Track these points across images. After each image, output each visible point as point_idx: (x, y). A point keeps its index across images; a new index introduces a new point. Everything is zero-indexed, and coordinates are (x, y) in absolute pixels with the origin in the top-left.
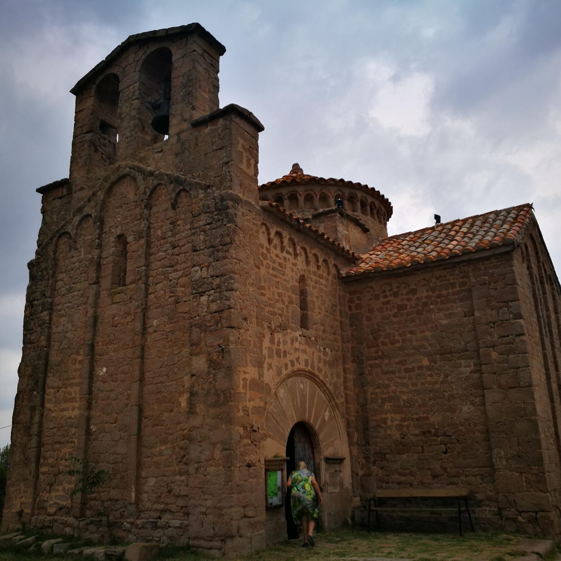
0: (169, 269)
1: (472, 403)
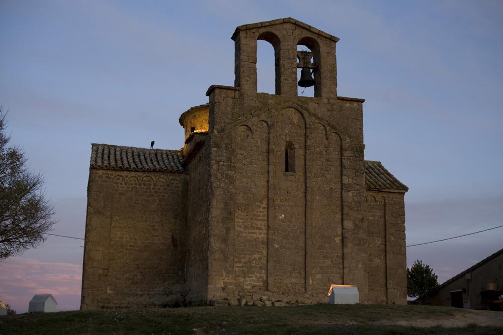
0: (326, 172)
1: (380, 259)
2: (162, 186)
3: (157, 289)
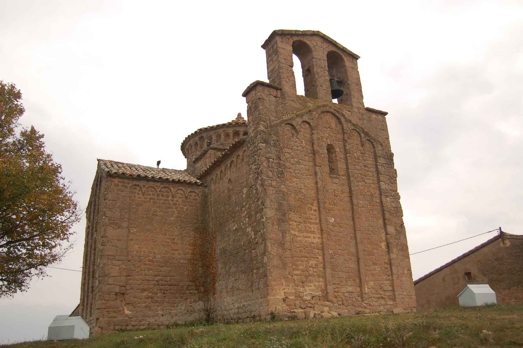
2: (180, 198)
3: (179, 307)
